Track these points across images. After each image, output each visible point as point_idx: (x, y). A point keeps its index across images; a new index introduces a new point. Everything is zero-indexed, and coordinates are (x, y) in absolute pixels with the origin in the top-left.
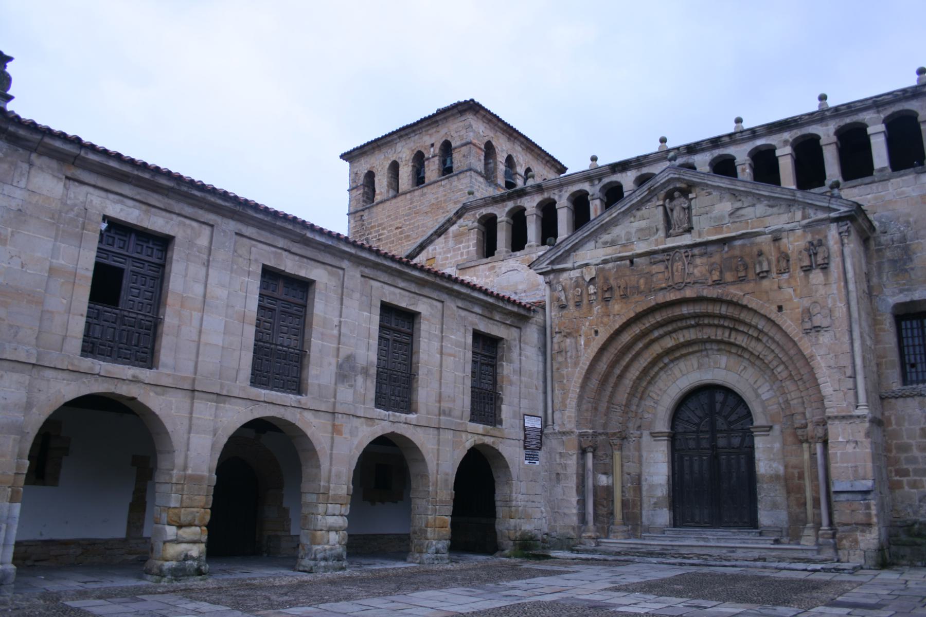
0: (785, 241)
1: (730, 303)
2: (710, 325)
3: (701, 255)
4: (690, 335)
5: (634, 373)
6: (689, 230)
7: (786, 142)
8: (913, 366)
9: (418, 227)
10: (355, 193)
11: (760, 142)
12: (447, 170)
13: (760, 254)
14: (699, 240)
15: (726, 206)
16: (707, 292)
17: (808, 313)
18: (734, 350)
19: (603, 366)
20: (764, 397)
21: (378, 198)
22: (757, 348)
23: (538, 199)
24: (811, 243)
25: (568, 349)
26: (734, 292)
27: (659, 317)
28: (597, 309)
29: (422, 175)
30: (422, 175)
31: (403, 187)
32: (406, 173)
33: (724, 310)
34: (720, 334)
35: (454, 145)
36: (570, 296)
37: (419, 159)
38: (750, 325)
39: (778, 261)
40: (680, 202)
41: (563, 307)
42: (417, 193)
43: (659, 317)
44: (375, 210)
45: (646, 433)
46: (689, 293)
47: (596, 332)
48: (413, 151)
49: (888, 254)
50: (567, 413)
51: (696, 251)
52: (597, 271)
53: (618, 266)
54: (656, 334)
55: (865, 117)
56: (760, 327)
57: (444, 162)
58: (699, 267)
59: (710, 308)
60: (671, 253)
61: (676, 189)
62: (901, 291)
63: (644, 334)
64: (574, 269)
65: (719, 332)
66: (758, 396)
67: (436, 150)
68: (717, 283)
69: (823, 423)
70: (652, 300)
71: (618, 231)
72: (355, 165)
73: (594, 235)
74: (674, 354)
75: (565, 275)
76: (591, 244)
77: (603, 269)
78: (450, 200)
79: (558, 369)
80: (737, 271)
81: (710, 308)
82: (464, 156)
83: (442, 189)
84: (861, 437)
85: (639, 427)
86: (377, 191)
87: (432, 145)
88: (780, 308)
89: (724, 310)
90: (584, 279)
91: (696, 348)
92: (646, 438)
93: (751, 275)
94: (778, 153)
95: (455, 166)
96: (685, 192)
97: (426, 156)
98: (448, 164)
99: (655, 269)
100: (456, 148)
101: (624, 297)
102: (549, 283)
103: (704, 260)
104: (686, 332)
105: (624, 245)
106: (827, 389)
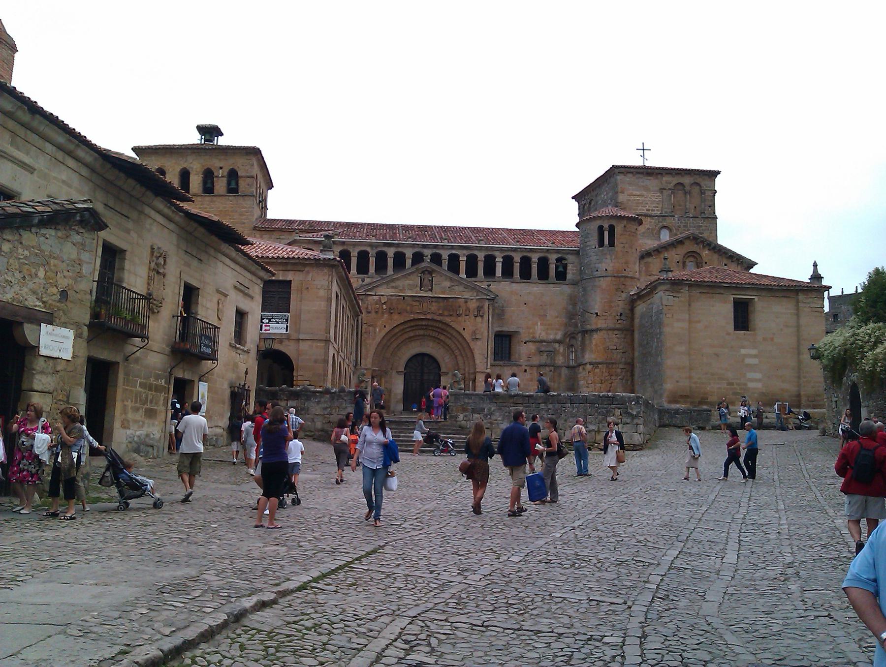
0: (469, 303)
1: (445, 324)
2: (431, 330)
3: (436, 302)
5: (395, 345)
6: (431, 290)
7: (464, 255)
8: (498, 354)
11: (454, 252)
12: (233, 190)
13: (460, 307)
14: (436, 296)
15: (447, 284)
16: (436, 317)
17: (474, 332)
18: (437, 341)
19: (385, 341)
20: (447, 361)
22: (448, 342)
24: (478, 306)
25: (371, 331)
26: (448, 320)
27: (412, 324)
28: (386, 316)
29: (209, 185)
30: (209, 185)
31: (194, 190)
33: (440, 325)
34: (435, 334)
36: (373, 308)
37: (208, 176)
38: (449, 333)
39: (466, 310)
41: (369, 312)
43: (412, 324)
46: (428, 317)
47: (385, 326)
48: (203, 166)
49: (496, 311)
50: (368, 360)
51: (434, 300)
52: (388, 298)
53: (398, 299)
54: (408, 330)
55: (497, 254)
56: (454, 334)
57: (229, 184)
58: (434, 307)
59: (435, 324)
60: (423, 298)
61: (426, 270)
62: (499, 326)
63: (403, 330)
64: (375, 295)
65: (434, 333)
66: (444, 360)
67: (225, 172)
68: (441, 315)
69: (475, 373)
70: (412, 316)
71: (399, 283)
72: (145, 158)
73: (387, 283)
74: (411, 339)
75: (371, 297)
76: (385, 286)
77: (390, 299)
78: (236, 212)
79: (364, 340)
80: (449, 311)
81: (435, 324)
82: (248, 185)
85: (391, 369)
87: (221, 168)
88: (464, 329)
89: (440, 325)
90: (381, 301)
91: (421, 337)
93: (455, 314)
94: (460, 259)
96: (430, 273)
97: (215, 174)
99: (415, 303)
101: (399, 313)
103: (436, 304)
104: (420, 331)
105: (400, 290)
106: (477, 362)
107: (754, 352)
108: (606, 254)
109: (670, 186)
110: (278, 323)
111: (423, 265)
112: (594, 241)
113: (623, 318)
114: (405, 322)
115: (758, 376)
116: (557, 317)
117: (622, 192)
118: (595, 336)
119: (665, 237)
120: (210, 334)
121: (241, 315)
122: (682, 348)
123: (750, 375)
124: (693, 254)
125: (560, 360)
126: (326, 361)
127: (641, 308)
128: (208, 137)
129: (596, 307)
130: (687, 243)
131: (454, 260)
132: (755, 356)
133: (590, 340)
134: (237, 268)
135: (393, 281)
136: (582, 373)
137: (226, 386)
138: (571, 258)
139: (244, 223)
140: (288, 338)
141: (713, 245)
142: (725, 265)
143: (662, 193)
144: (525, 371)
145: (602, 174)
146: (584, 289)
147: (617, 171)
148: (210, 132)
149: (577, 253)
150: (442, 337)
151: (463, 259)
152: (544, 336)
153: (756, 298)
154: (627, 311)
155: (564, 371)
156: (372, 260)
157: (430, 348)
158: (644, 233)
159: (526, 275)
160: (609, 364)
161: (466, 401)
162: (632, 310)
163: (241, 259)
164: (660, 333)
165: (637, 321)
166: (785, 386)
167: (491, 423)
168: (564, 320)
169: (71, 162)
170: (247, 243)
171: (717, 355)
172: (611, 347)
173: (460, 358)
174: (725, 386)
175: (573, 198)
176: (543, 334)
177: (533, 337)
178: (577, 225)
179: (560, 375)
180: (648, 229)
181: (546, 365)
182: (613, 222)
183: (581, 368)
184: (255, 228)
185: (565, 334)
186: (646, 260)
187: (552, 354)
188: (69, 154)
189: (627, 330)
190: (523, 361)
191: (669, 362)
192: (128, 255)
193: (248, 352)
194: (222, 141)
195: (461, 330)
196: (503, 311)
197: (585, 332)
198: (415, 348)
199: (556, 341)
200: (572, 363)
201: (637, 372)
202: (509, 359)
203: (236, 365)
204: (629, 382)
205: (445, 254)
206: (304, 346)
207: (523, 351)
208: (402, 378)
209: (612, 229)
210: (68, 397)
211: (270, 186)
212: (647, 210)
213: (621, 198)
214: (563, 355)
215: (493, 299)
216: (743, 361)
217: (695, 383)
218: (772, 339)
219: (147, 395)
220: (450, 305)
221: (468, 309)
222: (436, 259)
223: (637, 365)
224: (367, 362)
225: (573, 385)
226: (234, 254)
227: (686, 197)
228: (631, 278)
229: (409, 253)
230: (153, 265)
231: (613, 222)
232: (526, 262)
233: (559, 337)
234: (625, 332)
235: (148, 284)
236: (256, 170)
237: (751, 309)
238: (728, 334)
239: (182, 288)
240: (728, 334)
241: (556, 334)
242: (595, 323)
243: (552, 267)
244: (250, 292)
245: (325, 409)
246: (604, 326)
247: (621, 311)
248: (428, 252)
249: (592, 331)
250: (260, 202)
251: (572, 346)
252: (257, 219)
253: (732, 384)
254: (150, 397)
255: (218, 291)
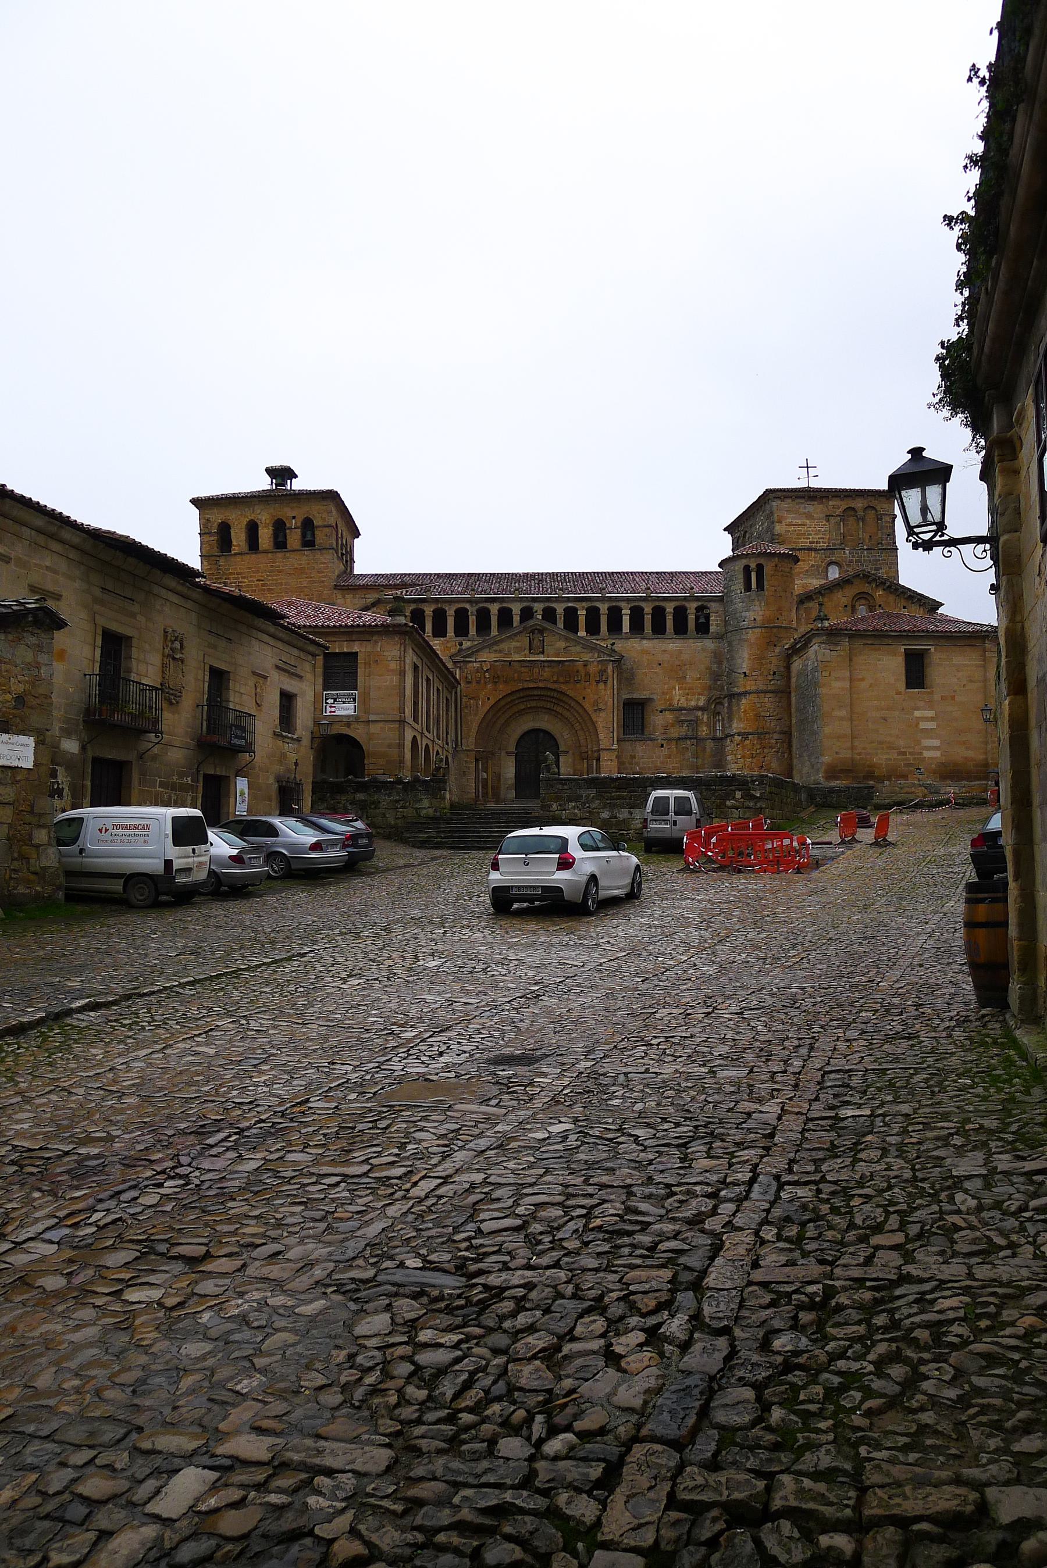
4: (533, 704)
6: (543, 652)
9: (281, 584)
10: (207, 538)
11: (570, 604)
12: (309, 543)
15: (562, 644)
21: (235, 550)
22: (567, 714)
23: (433, 607)
26: (564, 688)
32: (265, 536)
35: (315, 523)
37: (280, 527)
40: (538, 637)
41: (469, 682)
42: (279, 555)
44: (233, 559)
45: (503, 754)
46: (541, 685)
49: (625, 675)
55: (623, 604)
57: (304, 535)
58: (547, 673)
69: (599, 750)
70: (521, 685)
73: (490, 646)
74: (521, 713)
76: (487, 650)
83: (305, 558)
84: (614, 758)
86: (234, 543)
87: (294, 518)
89: (555, 695)
92: (503, 754)
95: (318, 541)
96: (541, 632)
98: (309, 538)
100: (318, 527)
101: (506, 682)
102: (460, 668)
106: (602, 737)
107: (931, 714)
108: (753, 600)
109: (838, 512)
110: (344, 703)
111: (531, 623)
112: (739, 586)
113: (776, 677)
114: (513, 693)
115: (936, 743)
116: (699, 679)
117: (780, 522)
118: (744, 701)
119: (834, 573)
120: (242, 724)
121: (287, 699)
122: (843, 713)
123: (927, 742)
124: (862, 596)
125: (703, 731)
126: (401, 746)
127: (797, 665)
128: (279, 481)
129: (745, 665)
130: (856, 581)
131: (571, 615)
132: (932, 719)
133: (738, 705)
134: (280, 644)
135: (496, 643)
136: (729, 747)
137: (271, 780)
138: (714, 606)
139: (323, 582)
140: (356, 719)
141: (888, 584)
142: (904, 607)
143: (828, 521)
144: (662, 746)
145: (755, 500)
146: (730, 644)
147: (771, 496)
148: (282, 474)
149: (720, 599)
150: (559, 709)
151: (582, 613)
152: (683, 703)
153: (933, 649)
154: (782, 669)
155: (710, 745)
156: (472, 619)
157: (544, 722)
158: (807, 571)
159: (659, 629)
160: (761, 735)
161: (560, 787)
162: (788, 668)
163: (281, 634)
164: (816, 695)
165: (793, 680)
166: (970, 754)
167: (590, 812)
168: (708, 682)
169: (56, 546)
170: (283, 617)
171: (885, 719)
172: (763, 714)
173: (580, 733)
174: (896, 756)
175: (725, 530)
176: (683, 700)
177: (670, 705)
178: (720, 565)
179: (704, 749)
180: (813, 566)
181: (685, 738)
182: (762, 561)
183: (728, 740)
184: (336, 587)
185: (710, 699)
186: (806, 605)
187: (695, 723)
188: (52, 536)
189: (782, 692)
190: (658, 734)
191: (827, 730)
192: (135, 642)
193: (299, 740)
194: (297, 485)
195: (580, 699)
196: (633, 674)
197: (731, 696)
198: (527, 723)
199: (698, 708)
200: (719, 734)
201: (795, 742)
202: (643, 733)
203: (283, 756)
204: (786, 755)
205: (560, 608)
206: (374, 729)
207: (658, 721)
208: (513, 759)
209: (760, 568)
210: (32, 806)
211: (356, 534)
212: (811, 543)
213: (778, 528)
214: (708, 725)
215: (618, 661)
216: (917, 725)
217: (859, 754)
218: (953, 698)
219: (170, 797)
220: (567, 671)
221: (588, 674)
222: (549, 615)
223: (795, 734)
224: (470, 742)
225: (720, 760)
226: (272, 629)
227: (858, 524)
228: (786, 628)
229: (516, 609)
230: (167, 651)
231: (762, 561)
232: (659, 613)
233: (701, 704)
234: (779, 695)
235: (163, 672)
236: (333, 517)
237: (926, 661)
238: (899, 693)
239: (207, 673)
240: (899, 693)
241: (698, 699)
242: (743, 685)
243: (691, 618)
244: (299, 671)
245: (397, 801)
246: (753, 688)
247: (773, 668)
248: (538, 607)
249: (740, 694)
250: (342, 554)
251: (719, 713)
252: (338, 576)
253: (904, 753)
254: (174, 797)
255: (254, 673)
